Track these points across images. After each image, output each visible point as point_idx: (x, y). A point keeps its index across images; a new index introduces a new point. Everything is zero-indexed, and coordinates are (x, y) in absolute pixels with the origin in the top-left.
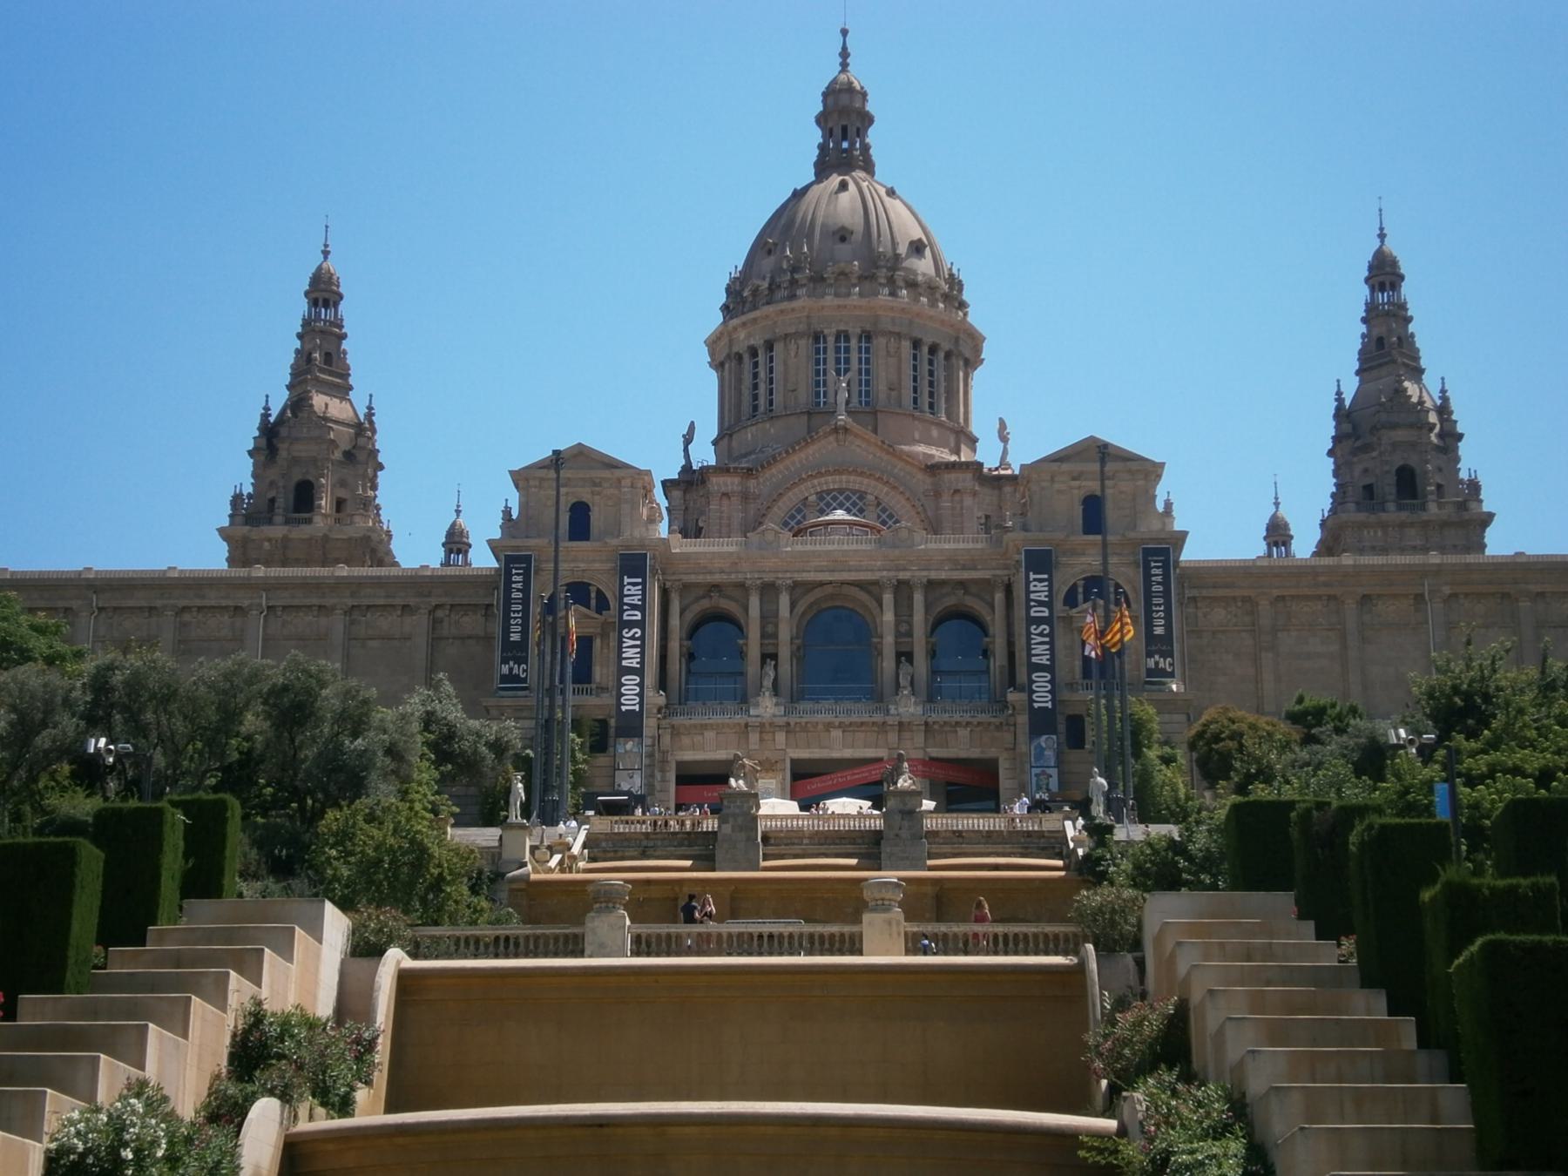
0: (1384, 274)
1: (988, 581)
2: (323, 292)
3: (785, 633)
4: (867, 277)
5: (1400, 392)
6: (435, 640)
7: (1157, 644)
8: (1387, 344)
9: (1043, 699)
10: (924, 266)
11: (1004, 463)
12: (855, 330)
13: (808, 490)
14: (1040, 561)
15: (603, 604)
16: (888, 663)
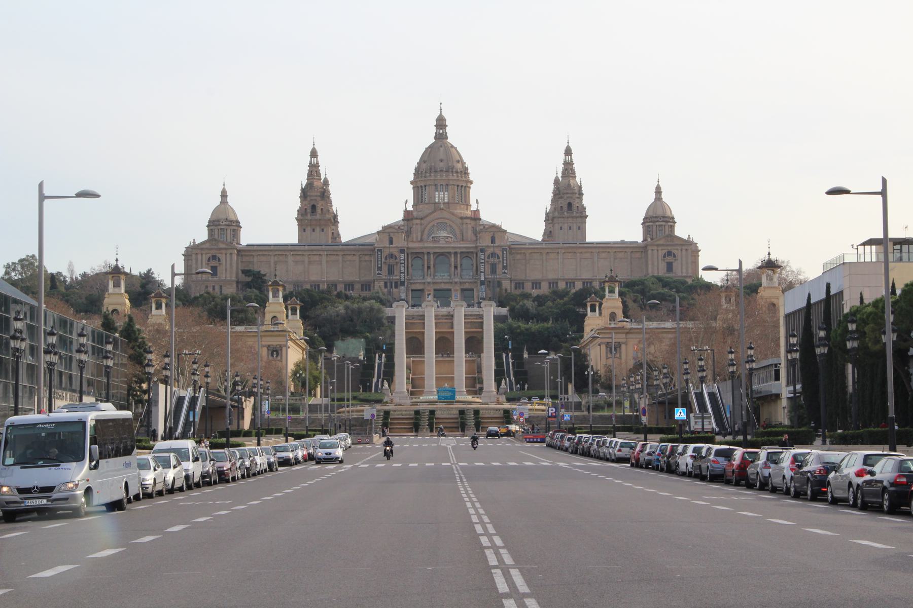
0: (568, 152)
1: (472, 252)
2: (314, 154)
3: (432, 263)
4: (447, 171)
5: (569, 185)
6: (360, 261)
7: (505, 267)
8: (568, 169)
9: (482, 279)
10: (459, 166)
11: (477, 211)
12: (444, 184)
13: (435, 223)
14: (483, 251)
15: (396, 258)
16: (453, 269)
